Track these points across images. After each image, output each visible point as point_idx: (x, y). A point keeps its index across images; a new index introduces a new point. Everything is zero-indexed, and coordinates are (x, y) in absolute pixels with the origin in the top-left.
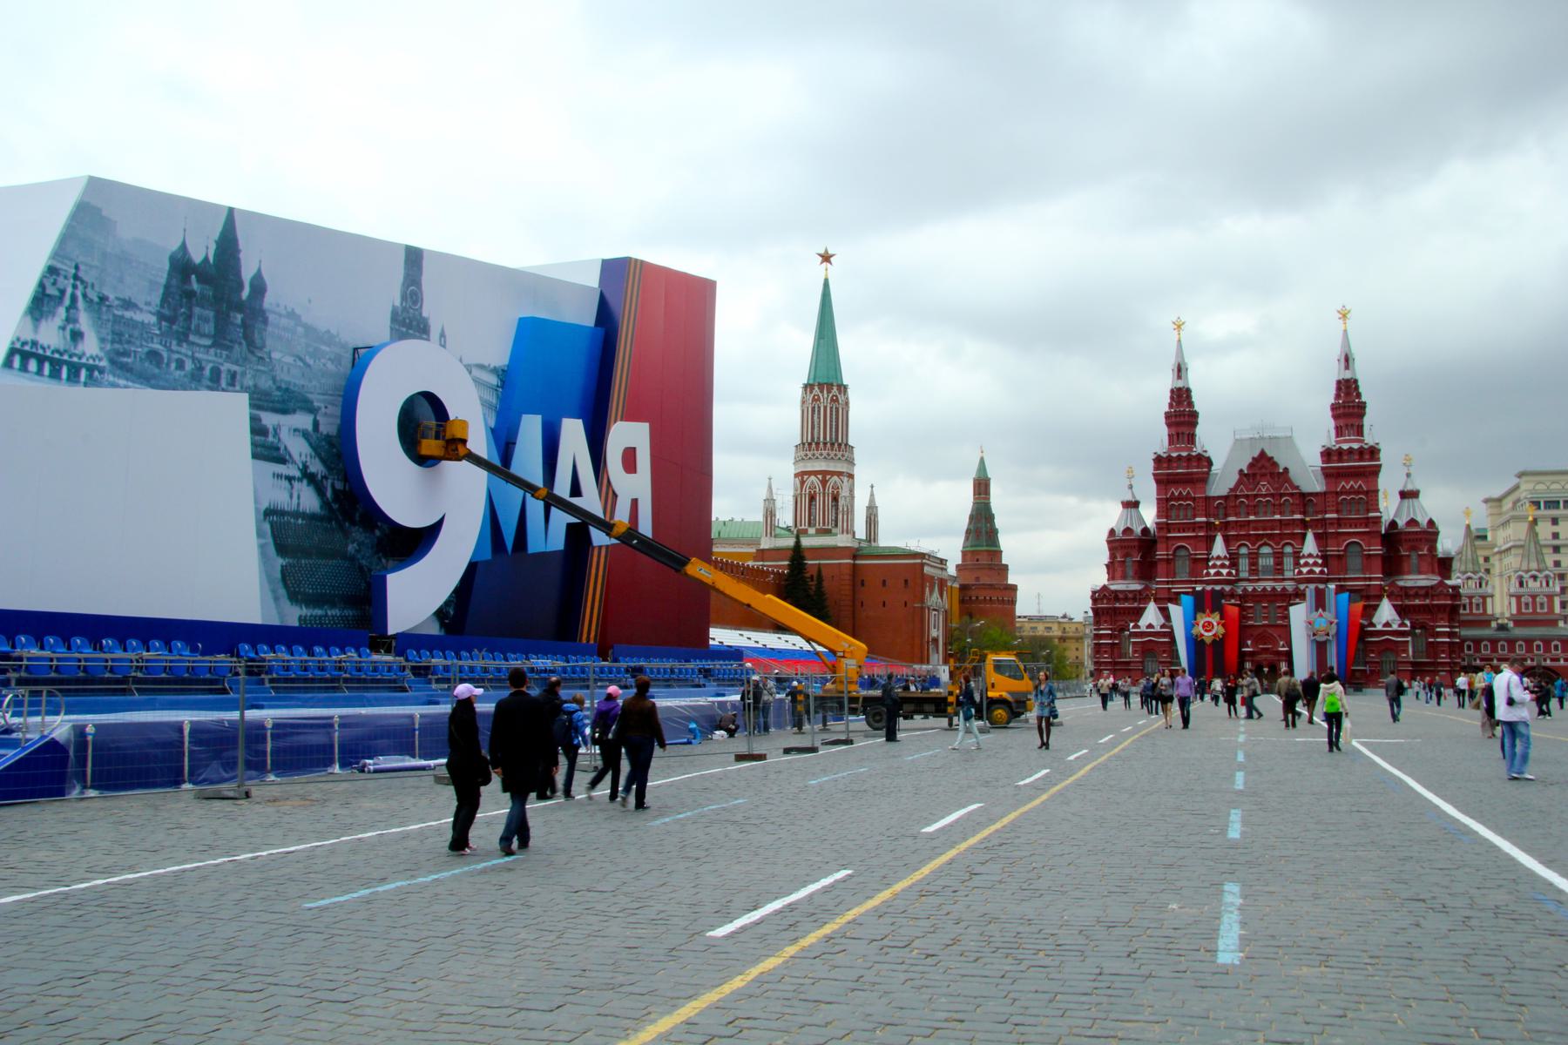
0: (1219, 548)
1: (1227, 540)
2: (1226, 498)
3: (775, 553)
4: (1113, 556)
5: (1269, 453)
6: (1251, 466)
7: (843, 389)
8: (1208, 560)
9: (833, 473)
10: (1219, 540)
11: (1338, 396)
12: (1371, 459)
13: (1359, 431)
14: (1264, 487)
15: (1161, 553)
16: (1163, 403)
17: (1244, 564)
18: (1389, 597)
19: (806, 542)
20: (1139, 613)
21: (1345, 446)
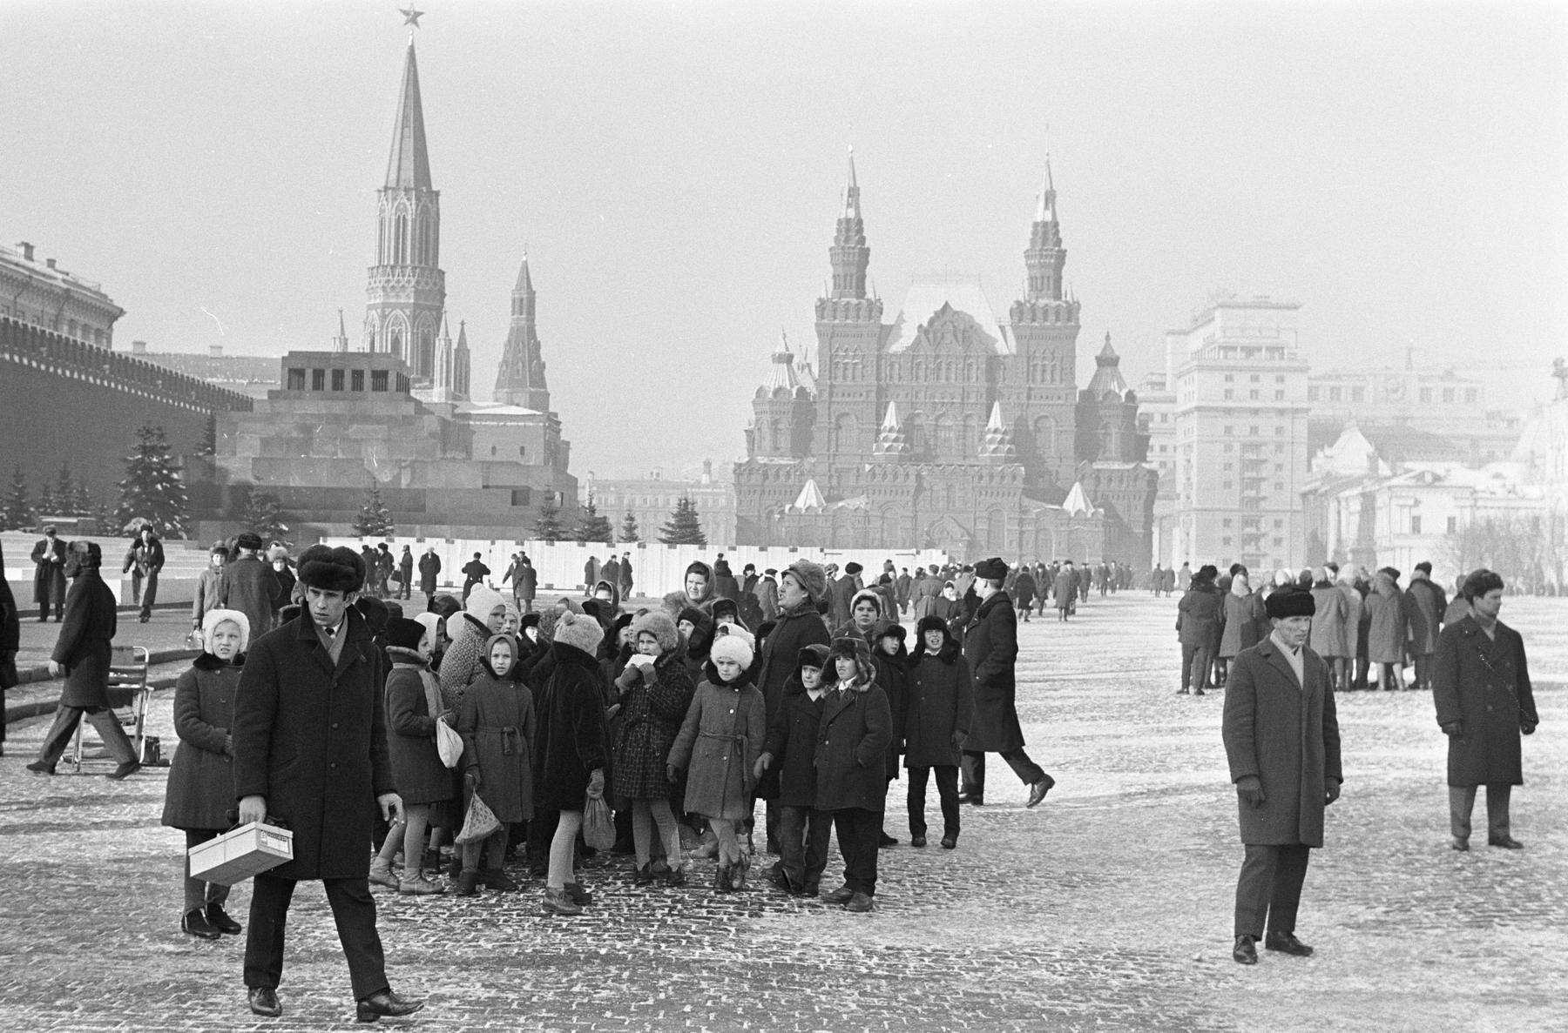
0: (891, 419)
2: (903, 355)
5: (955, 307)
6: (931, 322)
8: (878, 432)
10: (892, 406)
11: (1033, 241)
12: (1069, 320)
18: (1082, 480)
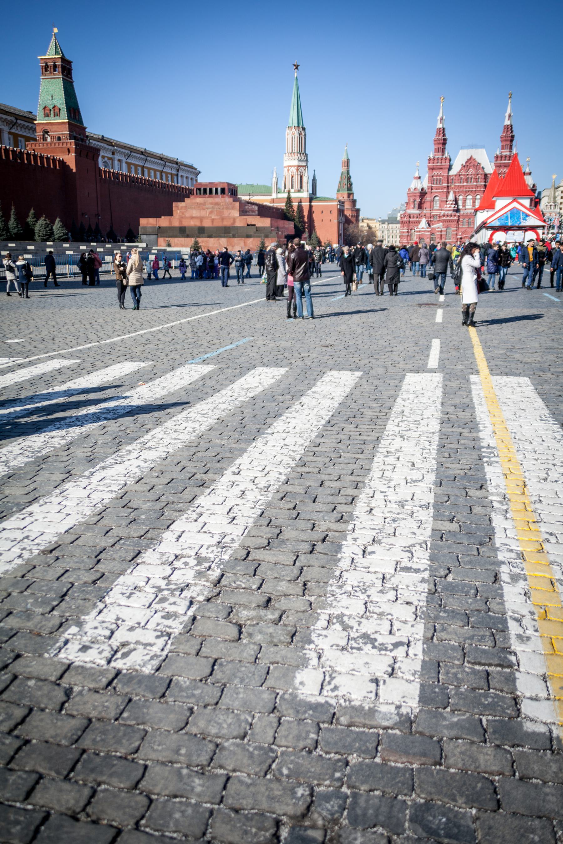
0: (451, 197)
1: (455, 193)
2: (456, 175)
3: (279, 200)
4: (409, 200)
6: (466, 162)
7: (304, 129)
9: (301, 166)
13: (511, 147)
14: (472, 171)
15: (428, 198)
16: (433, 136)
17: (460, 203)
19: (293, 195)
20: (419, 222)
21: (504, 154)
